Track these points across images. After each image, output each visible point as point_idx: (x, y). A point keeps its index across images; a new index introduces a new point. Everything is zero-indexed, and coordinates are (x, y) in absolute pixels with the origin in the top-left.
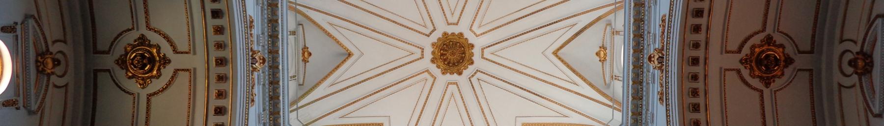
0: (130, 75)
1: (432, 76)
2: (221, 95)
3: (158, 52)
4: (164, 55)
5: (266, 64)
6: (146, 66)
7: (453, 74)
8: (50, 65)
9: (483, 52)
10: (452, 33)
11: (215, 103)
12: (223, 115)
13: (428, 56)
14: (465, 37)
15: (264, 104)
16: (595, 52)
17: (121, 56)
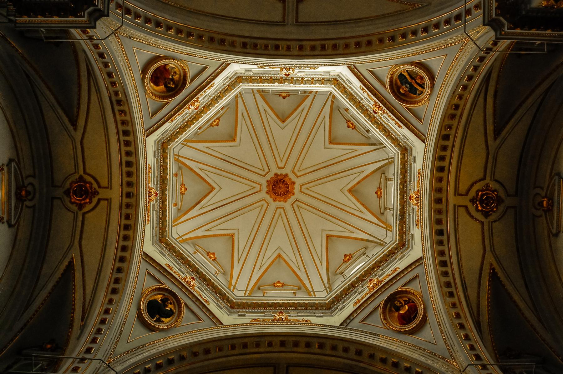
2: (440, 180)
3: (477, 207)
4: (473, 205)
5: (408, 197)
8: (545, 203)
15: (411, 169)
16: (187, 191)
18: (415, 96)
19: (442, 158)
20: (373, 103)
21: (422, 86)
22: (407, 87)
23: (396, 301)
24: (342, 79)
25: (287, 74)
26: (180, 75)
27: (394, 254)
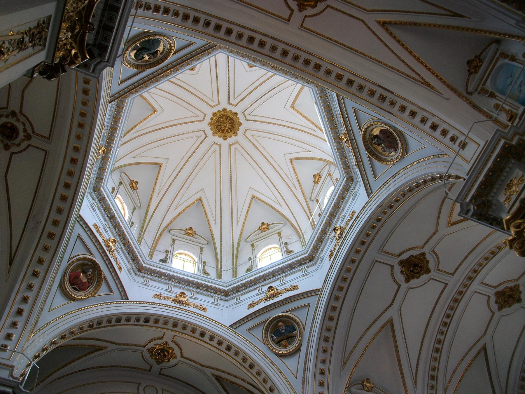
1: (235, 143)
3: (160, 345)
6: (165, 354)
7: (239, 129)
9: (231, 104)
10: (211, 119)
12: (205, 334)
13: (220, 140)
14: (217, 112)
21: (278, 343)
22: (282, 329)
23: (92, 270)
26: (381, 154)
27: (133, 260)
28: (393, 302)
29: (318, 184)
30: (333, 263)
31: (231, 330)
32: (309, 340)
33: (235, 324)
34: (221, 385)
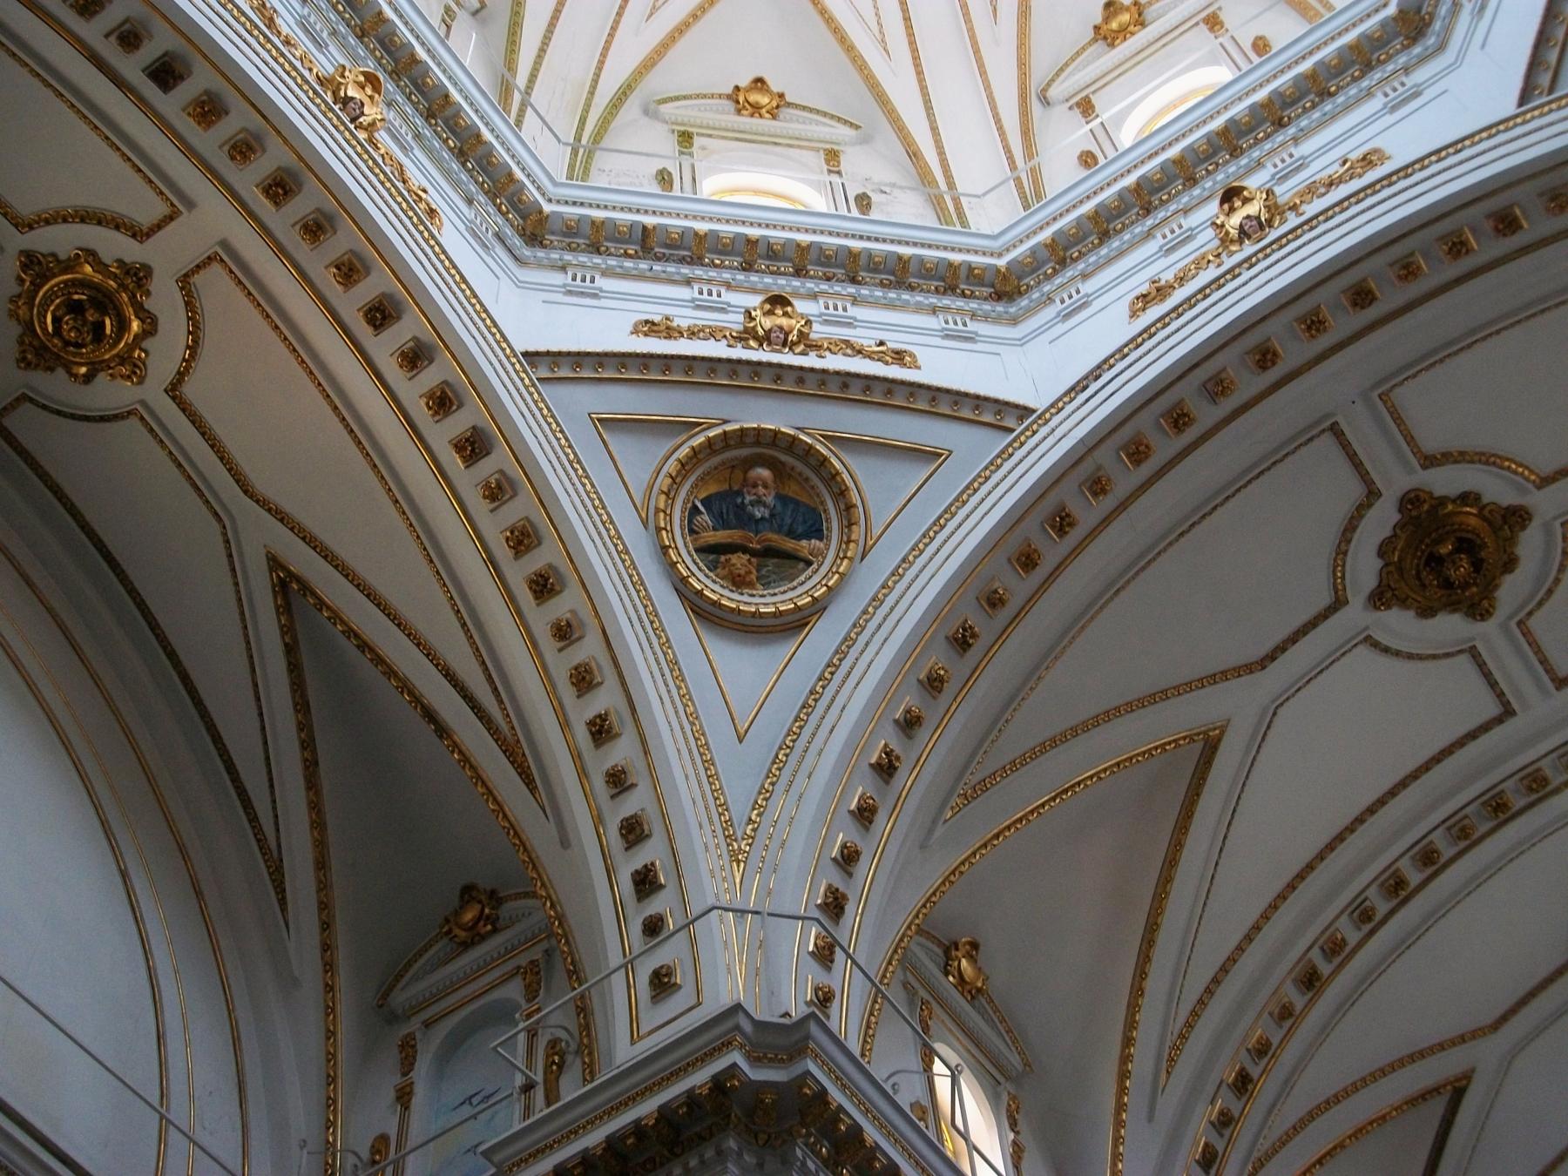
0: (83, 370)
2: (349, 271)
4: (121, 263)
6: (103, 323)
11: (351, 304)
12: (399, 318)
15: (456, 184)
17: (21, 343)
18: (703, 495)
19: (415, 358)
20: (819, 331)
21: (712, 553)
22: (759, 502)
24: (986, 318)
25: (1238, 203)
28: (1272, 657)
29: (1112, 45)
30: (1135, 342)
31: (525, 371)
32: (877, 601)
33: (555, 357)
34: (287, 630)
